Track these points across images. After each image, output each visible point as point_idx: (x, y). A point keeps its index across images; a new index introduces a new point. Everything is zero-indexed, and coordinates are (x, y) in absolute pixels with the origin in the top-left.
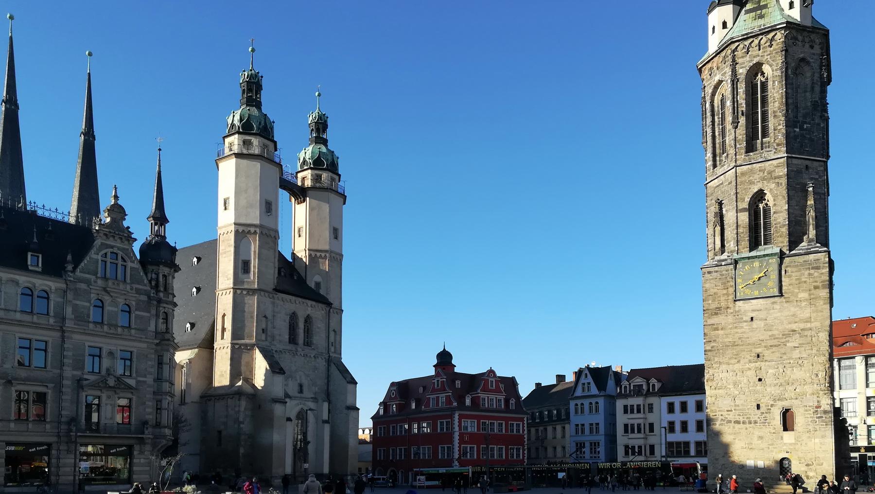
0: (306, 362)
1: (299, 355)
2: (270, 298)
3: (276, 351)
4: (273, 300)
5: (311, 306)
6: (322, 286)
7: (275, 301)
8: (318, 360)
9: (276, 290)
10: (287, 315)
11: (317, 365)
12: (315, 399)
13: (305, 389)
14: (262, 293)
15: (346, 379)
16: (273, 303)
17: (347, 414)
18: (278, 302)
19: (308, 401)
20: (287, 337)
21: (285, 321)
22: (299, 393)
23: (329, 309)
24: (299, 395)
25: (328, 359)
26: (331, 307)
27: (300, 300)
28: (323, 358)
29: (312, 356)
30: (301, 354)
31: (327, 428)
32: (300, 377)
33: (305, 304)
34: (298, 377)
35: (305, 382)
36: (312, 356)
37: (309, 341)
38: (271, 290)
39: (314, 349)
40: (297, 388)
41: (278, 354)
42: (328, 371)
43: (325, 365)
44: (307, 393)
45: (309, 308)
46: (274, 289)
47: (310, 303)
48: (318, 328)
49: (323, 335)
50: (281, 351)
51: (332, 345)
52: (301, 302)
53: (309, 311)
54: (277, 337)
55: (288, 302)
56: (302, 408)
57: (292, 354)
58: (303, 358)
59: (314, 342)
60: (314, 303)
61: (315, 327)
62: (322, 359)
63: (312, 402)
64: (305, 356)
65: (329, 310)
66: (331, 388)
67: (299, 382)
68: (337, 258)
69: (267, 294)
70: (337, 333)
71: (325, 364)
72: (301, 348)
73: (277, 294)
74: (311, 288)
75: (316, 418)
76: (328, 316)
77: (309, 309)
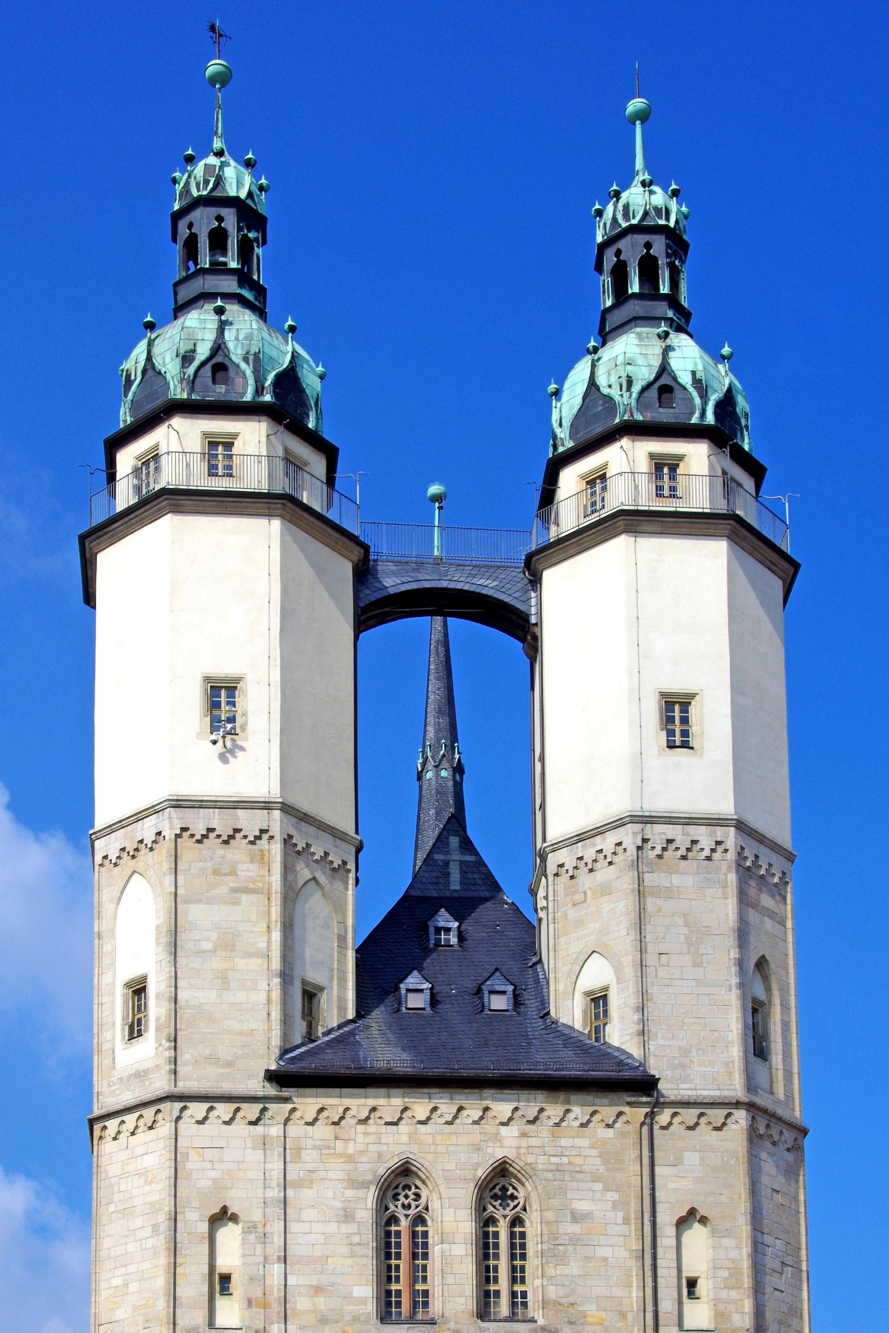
6: (615, 1002)
10: (365, 1185)
14: (198, 1109)
16: (264, 1143)
21: (347, 1216)
38: (257, 1086)
46: (272, 1077)
48: (576, 1218)
69: (224, 1110)
73: (287, 1100)
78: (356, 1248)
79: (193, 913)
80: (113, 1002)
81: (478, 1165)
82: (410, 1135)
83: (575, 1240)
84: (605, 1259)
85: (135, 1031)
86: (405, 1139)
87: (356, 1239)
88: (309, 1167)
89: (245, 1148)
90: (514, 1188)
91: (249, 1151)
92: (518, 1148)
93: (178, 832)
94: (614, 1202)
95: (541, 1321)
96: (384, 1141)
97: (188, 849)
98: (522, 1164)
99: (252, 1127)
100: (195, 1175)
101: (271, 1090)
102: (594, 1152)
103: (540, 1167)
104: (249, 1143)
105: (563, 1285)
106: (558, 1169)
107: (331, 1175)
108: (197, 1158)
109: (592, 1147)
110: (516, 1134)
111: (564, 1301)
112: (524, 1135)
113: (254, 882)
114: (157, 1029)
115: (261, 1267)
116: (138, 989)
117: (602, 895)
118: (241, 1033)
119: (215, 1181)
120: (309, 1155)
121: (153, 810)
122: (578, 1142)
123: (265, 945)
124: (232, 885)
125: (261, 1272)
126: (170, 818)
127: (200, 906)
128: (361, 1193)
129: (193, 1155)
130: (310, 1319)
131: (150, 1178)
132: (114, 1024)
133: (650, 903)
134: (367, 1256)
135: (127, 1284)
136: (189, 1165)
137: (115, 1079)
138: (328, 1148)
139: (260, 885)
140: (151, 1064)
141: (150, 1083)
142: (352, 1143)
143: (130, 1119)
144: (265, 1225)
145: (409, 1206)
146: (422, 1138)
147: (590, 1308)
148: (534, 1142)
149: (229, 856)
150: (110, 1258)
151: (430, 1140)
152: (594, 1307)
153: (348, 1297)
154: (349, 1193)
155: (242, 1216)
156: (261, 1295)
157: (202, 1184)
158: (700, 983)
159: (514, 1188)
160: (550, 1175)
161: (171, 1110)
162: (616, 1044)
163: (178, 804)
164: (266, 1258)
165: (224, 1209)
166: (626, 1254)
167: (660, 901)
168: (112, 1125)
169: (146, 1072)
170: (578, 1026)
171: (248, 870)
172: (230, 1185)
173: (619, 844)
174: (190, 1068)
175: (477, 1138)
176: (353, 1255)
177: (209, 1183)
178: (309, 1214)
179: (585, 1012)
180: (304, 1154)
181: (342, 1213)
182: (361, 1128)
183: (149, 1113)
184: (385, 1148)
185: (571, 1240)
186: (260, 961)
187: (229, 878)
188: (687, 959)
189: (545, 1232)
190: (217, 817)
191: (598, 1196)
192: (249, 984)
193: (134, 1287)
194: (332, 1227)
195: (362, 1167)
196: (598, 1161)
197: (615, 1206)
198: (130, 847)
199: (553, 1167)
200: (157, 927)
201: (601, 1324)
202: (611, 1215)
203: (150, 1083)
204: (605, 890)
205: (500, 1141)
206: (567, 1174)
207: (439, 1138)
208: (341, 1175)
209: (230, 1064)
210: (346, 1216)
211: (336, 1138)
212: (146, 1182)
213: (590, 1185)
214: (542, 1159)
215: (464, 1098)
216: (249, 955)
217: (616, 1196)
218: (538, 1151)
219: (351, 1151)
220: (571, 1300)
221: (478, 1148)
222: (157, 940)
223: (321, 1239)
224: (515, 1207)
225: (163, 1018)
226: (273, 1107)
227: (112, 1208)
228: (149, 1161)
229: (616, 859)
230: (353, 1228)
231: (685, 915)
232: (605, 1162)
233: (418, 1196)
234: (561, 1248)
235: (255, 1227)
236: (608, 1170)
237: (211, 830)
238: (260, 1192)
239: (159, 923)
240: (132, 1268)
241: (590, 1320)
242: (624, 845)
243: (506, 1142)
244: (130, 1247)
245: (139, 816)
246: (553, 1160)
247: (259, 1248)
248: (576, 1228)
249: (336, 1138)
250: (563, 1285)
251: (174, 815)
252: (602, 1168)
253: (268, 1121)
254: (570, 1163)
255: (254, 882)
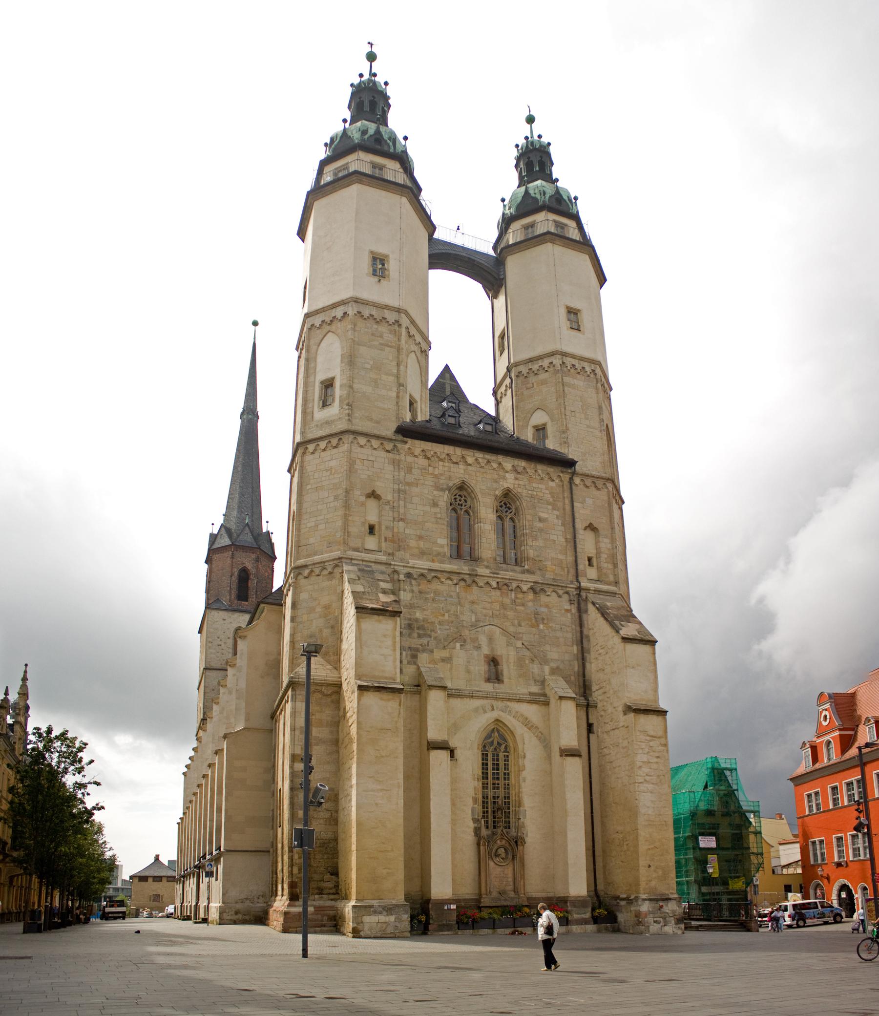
0: (507, 601)
1: (481, 584)
2: (388, 451)
3: (409, 575)
4: (397, 457)
5: (515, 469)
6: (550, 430)
7: (402, 457)
8: (543, 598)
9: (407, 432)
10: (443, 490)
11: (544, 610)
12: (542, 700)
13: (508, 670)
14: (362, 441)
15: (618, 632)
16: (396, 464)
17: (627, 727)
18: (410, 459)
19: (519, 701)
20: (443, 542)
21: (435, 504)
22: (488, 680)
23: (567, 477)
24: (489, 687)
25: (579, 595)
26: (574, 473)
27: (479, 455)
28: (561, 592)
29: (525, 587)
30: (488, 583)
31: (574, 768)
32: (491, 640)
33: (495, 465)
34: (483, 640)
35: (508, 655)
36: (525, 587)
37: (519, 554)
39: (529, 572)
40: (480, 668)
41: (413, 582)
42: (581, 625)
43: (567, 611)
44: (513, 683)
45: (507, 475)
47: (508, 463)
48: (541, 520)
49: (558, 535)
50: (422, 575)
51: (590, 564)
52: (480, 460)
53: (509, 481)
54: (413, 543)
55: (441, 460)
56: (497, 720)
57: (462, 584)
58: (498, 593)
59: (531, 553)
60: (522, 463)
61: (529, 517)
62: (560, 597)
63: (529, 702)
64: (503, 586)
65: (571, 479)
66: (592, 668)
67: (486, 650)
68: (583, 368)
69: (375, 443)
70: (601, 532)
71: (567, 607)
72: (487, 567)
73: (406, 442)
74: (527, 441)
75: (545, 742)
76: (567, 494)
77: (510, 476)
78: (439, 520)
79: (363, 350)
80: (314, 390)
81: (496, 489)
82: (464, 470)
83: (541, 530)
84: (554, 541)
85: (325, 404)
86: (462, 471)
87: (439, 516)
88: (416, 477)
89: (384, 463)
90: (510, 504)
91: (386, 465)
92: (514, 484)
93: (356, 313)
94: (557, 515)
95: (526, 567)
96: (452, 470)
97: (361, 324)
98: (516, 492)
99: (388, 454)
100: (359, 472)
101: (400, 437)
102: (547, 492)
103: (524, 494)
104: (387, 461)
105: (536, 550)
106: (532, 497)
107: (427, 483)
108: (360, 464)
109: (546, 489)
110: (513, 478)
111: (537, 559)
112: (516, 479)
113: (391, 343)
114: (340, 401)
115: (392, 523)
116: (328, 385)
117: (542, 385)
118: (384, 409)
119: (369, 476)
120: (416, 471)
121: (343, 303)
122: (540, 486)
123: (396, 371)
124: (381, 342)
125: (392, 525)
126: (352, 306)
127: (365, 348)
128: (441, 493)
129: (358, 461)
130: (416, 551)
131: (333, 472)
132: (313, 400)
133: (566, 389)
134: (444, 524)
135: (317, 526)
136: (356, 467)
137: (313, 425)
138: (425, 469)
139: (394, 345)
140: (337, 418)
141: (335, 426)
142: (437, 469)
143: (323, 444)
144: (393, 503)
145: (462, 505)
146: (470, 472)
147: (549, 563)
148: (521, 483)
149: (380, 329)
150: (306, 513)
151: (474, 473)
152: (550, 563)
153: (435, 543)
154: (436, 493)
155: (383, 497)
156: (391, 536)
157: (363, 476)
158: (588, 426)
159: (510, 504)
160: (529, 499)
161: (348, 439)
162: (551, 448)
163: (356, 301)
164: (394, 518)
165: (374, 491)
166: (563, 540)
167: (570, 389)
168: (311, 447)
169: (333, 421)
170: (529, 441)
171: (388, 337)
172: (376, 479)
173: (551, 363)
174: (358, 420)
175: (495, 476)
176: (437, 523)
177: (366, 477)
178: (416, 500)
179: (533, 435)
180: (413, 470)
181: (432, 502)
182: (441, 463)
183: (334, 441)
184: (452, 474)
185: (539, 529)
186: (393, 378)
187: (379, 338)
188: (583, 416)
189: (527, 524)
190: (375, 310)
191: (550, 512)
192: (388, 387)
193: (322, 527)
194: (427, 508)
195: (442, 481)
196: (549, 496)
197: (557, 517)
198: (328, 320)
199: (530, 496)
200: (342, 355)
201: (552, 572)
202: (556, 521)
203: (335, 426)
204: (544, 382)
205: (506, 479)
206: (536, 500)
207: (478, 474)
208: (432, 484)
209: (378, 422)
210: (434, 504)
211: (429, 466)
212: (331, 474)
213: (546, 506)
214: (524, 491)
215: (488, 456)
216: (387, 374)
217: (558, 513)
218: (522, 487)
219: (436, 473)
220: (540, 559)
221: (496, 481)
222: (341, 360)
223: (422, 513)
224: (511, 513)
225: (345, 396)
226: (399, 445)
227: (309, 487)
228: (333, 463)
229: (549, 370)
230: (438, 510)
231: (581, 397)
232: (553, 497)
233: (466, 501)
234: (535, 533)
235: (389, 502)
236: (554, 500)
237: (372, 316)
238: (391, 485)
239: (343, 353)
240: (321, 517)
241: (548, 569)
242: (554, 363)
243: (509, 481)
244: (320, 507)
245: (334, 306)
246: (530, 492)
247: (391, 512)
248: (540, 525)
249: (429, 466)
250: (536, 550)
251: (354, 305)
252: (551, 499)
253: (396, 452)
254: (537, 495)
255: (391, 343)
